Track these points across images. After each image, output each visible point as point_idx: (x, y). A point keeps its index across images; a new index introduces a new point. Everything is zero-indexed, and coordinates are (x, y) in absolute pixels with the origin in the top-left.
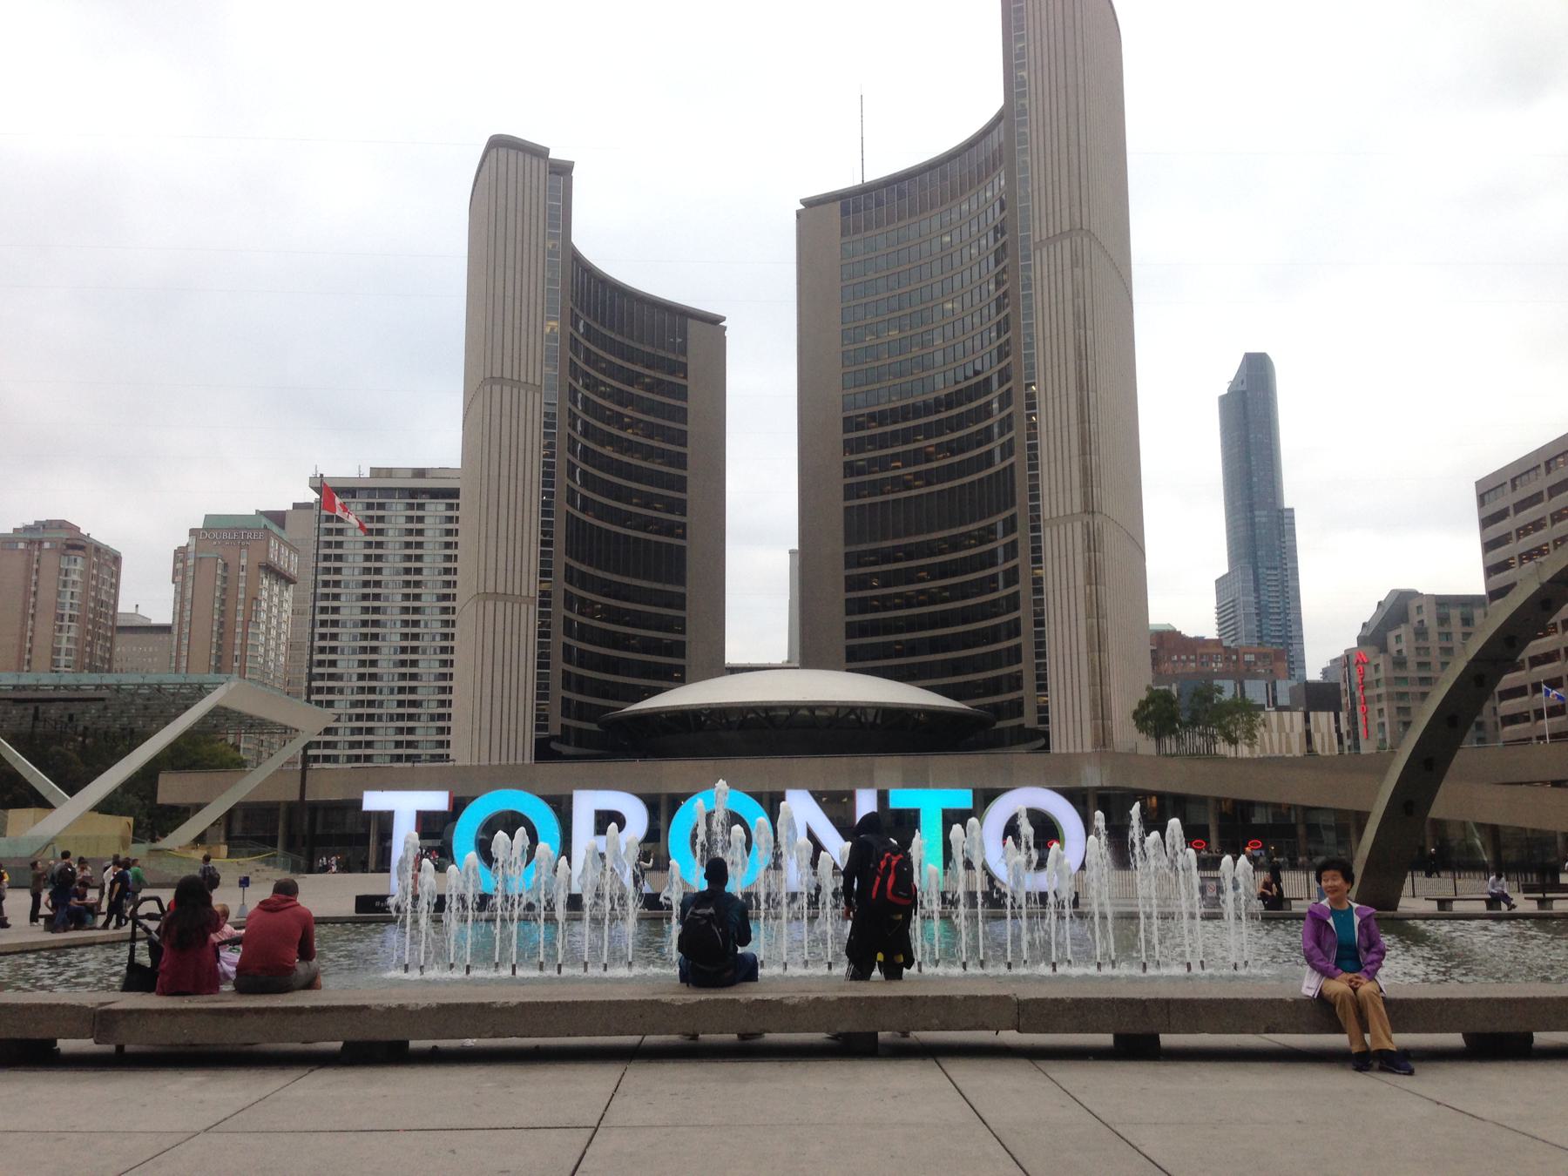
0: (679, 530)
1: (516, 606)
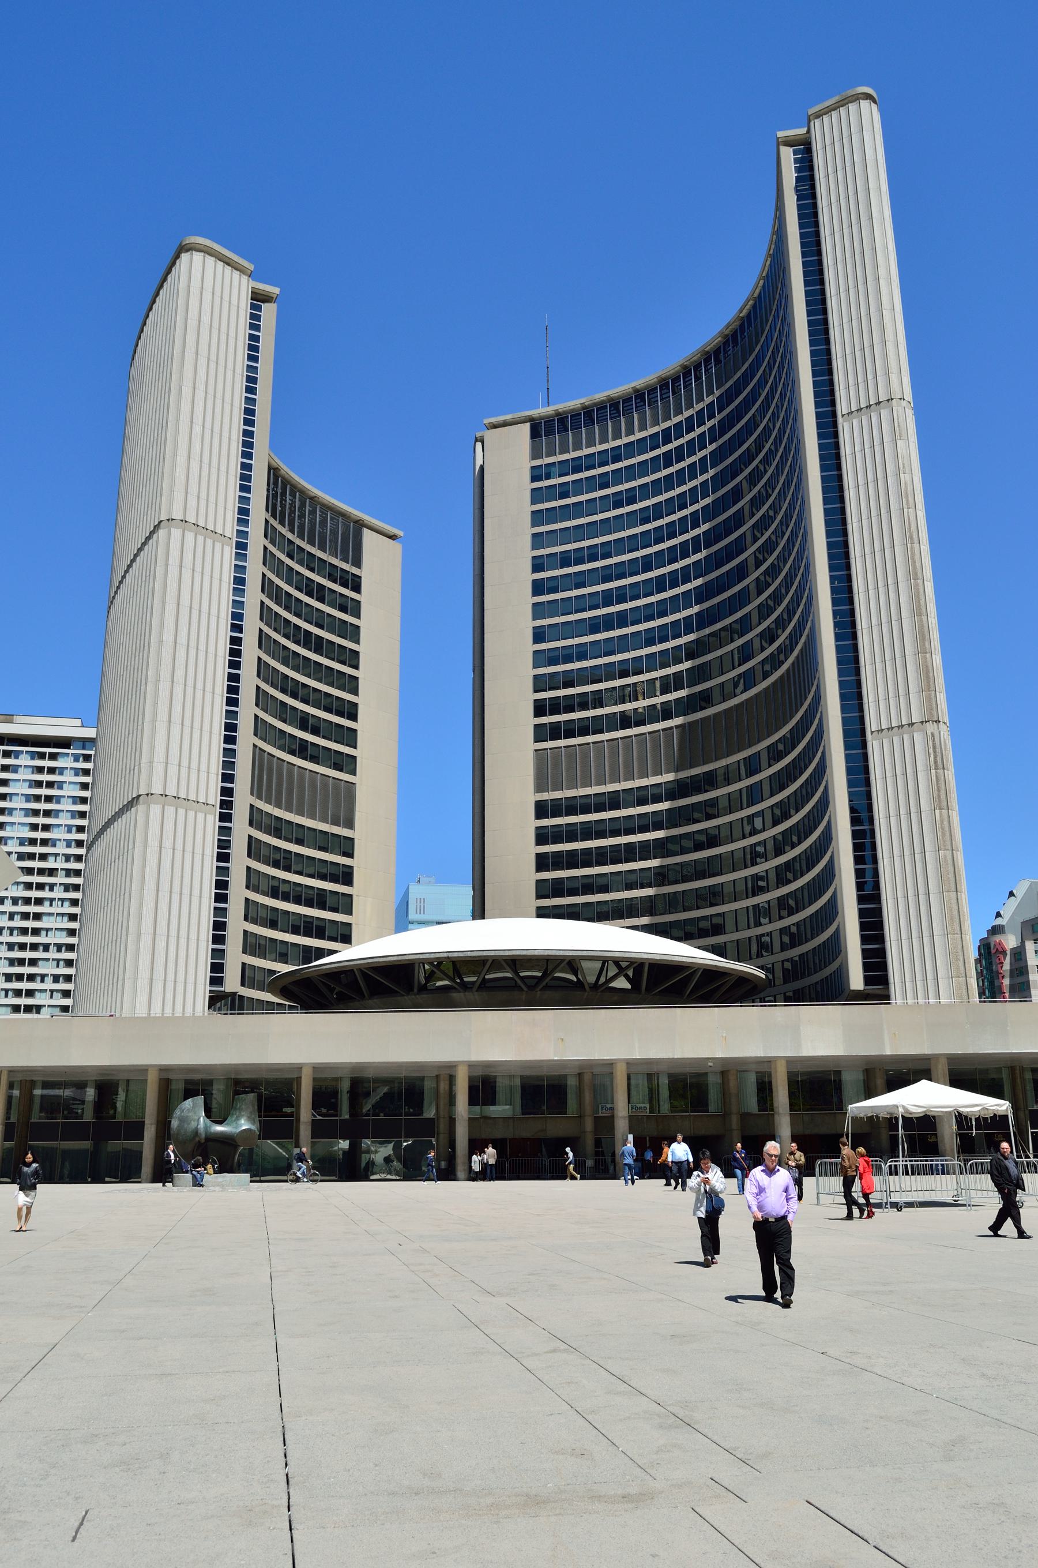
1: (191, 814)
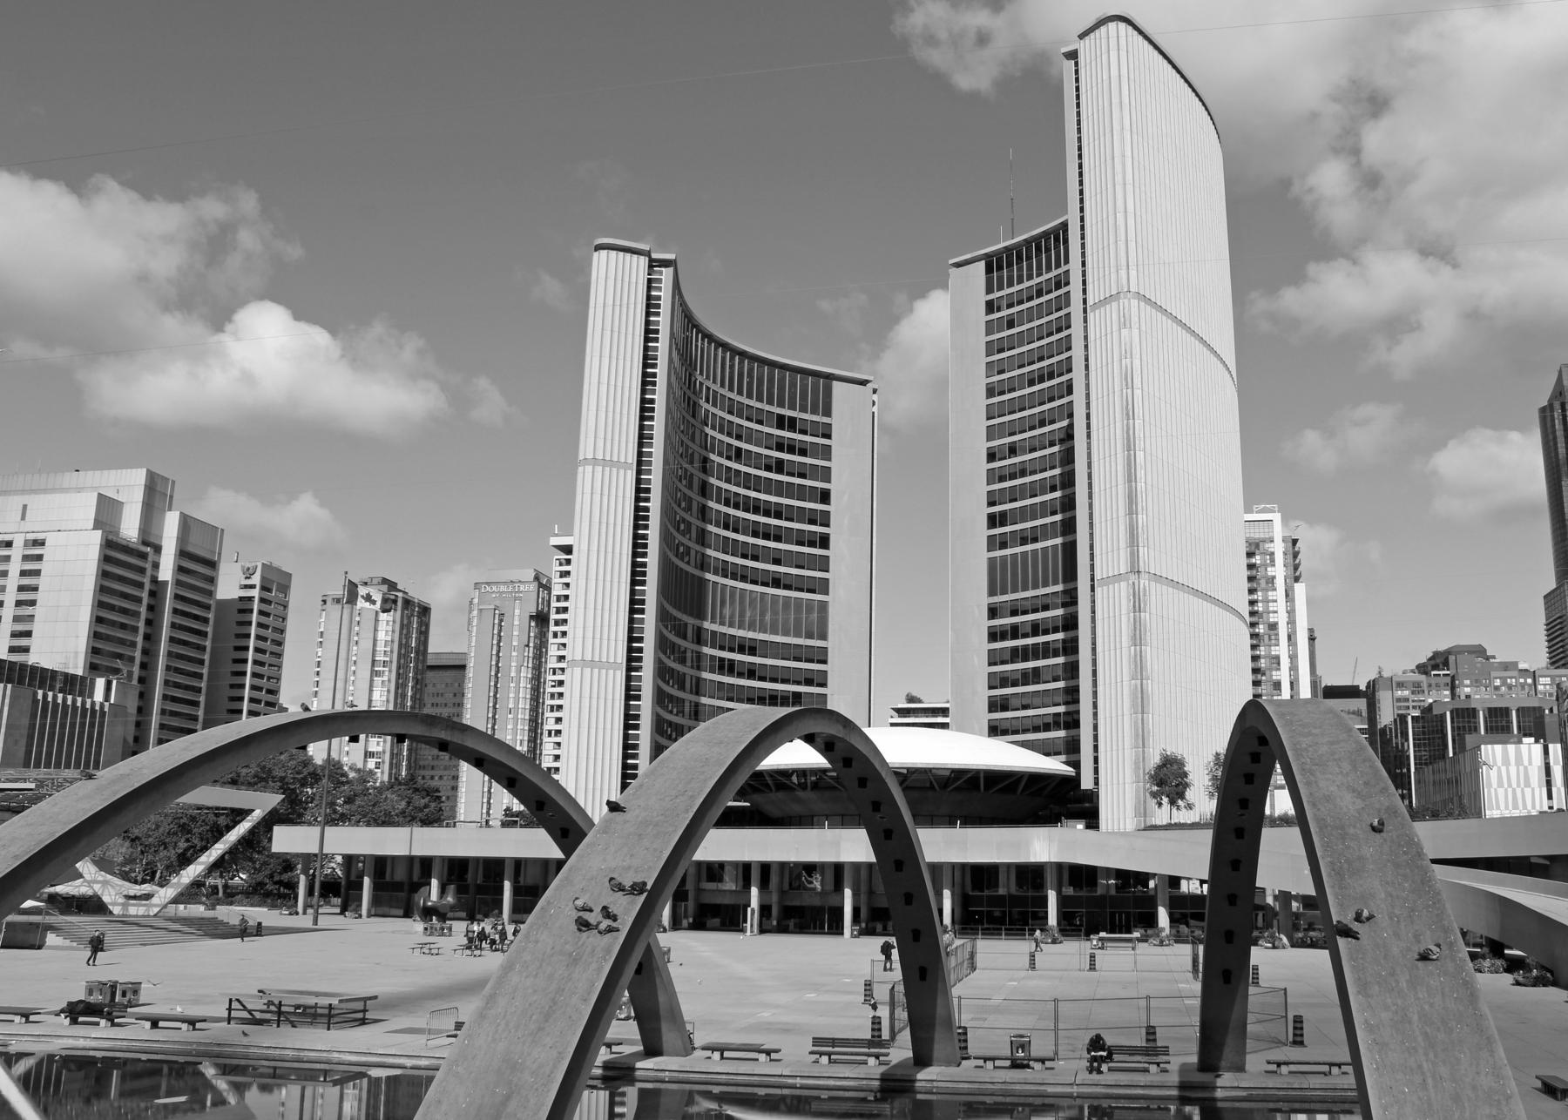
0: (823, 586)
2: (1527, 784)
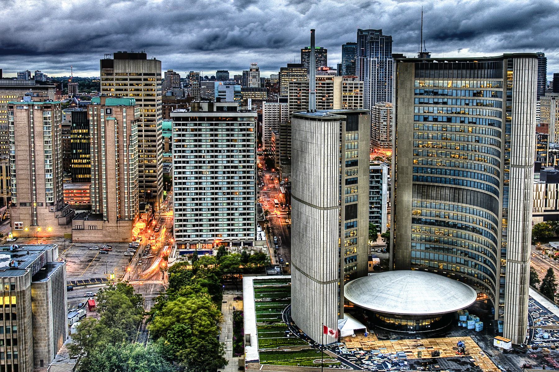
2: (539, 198)
